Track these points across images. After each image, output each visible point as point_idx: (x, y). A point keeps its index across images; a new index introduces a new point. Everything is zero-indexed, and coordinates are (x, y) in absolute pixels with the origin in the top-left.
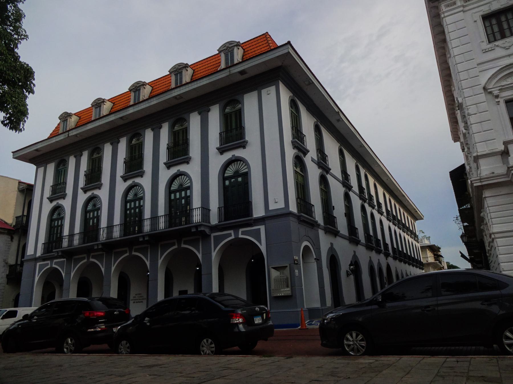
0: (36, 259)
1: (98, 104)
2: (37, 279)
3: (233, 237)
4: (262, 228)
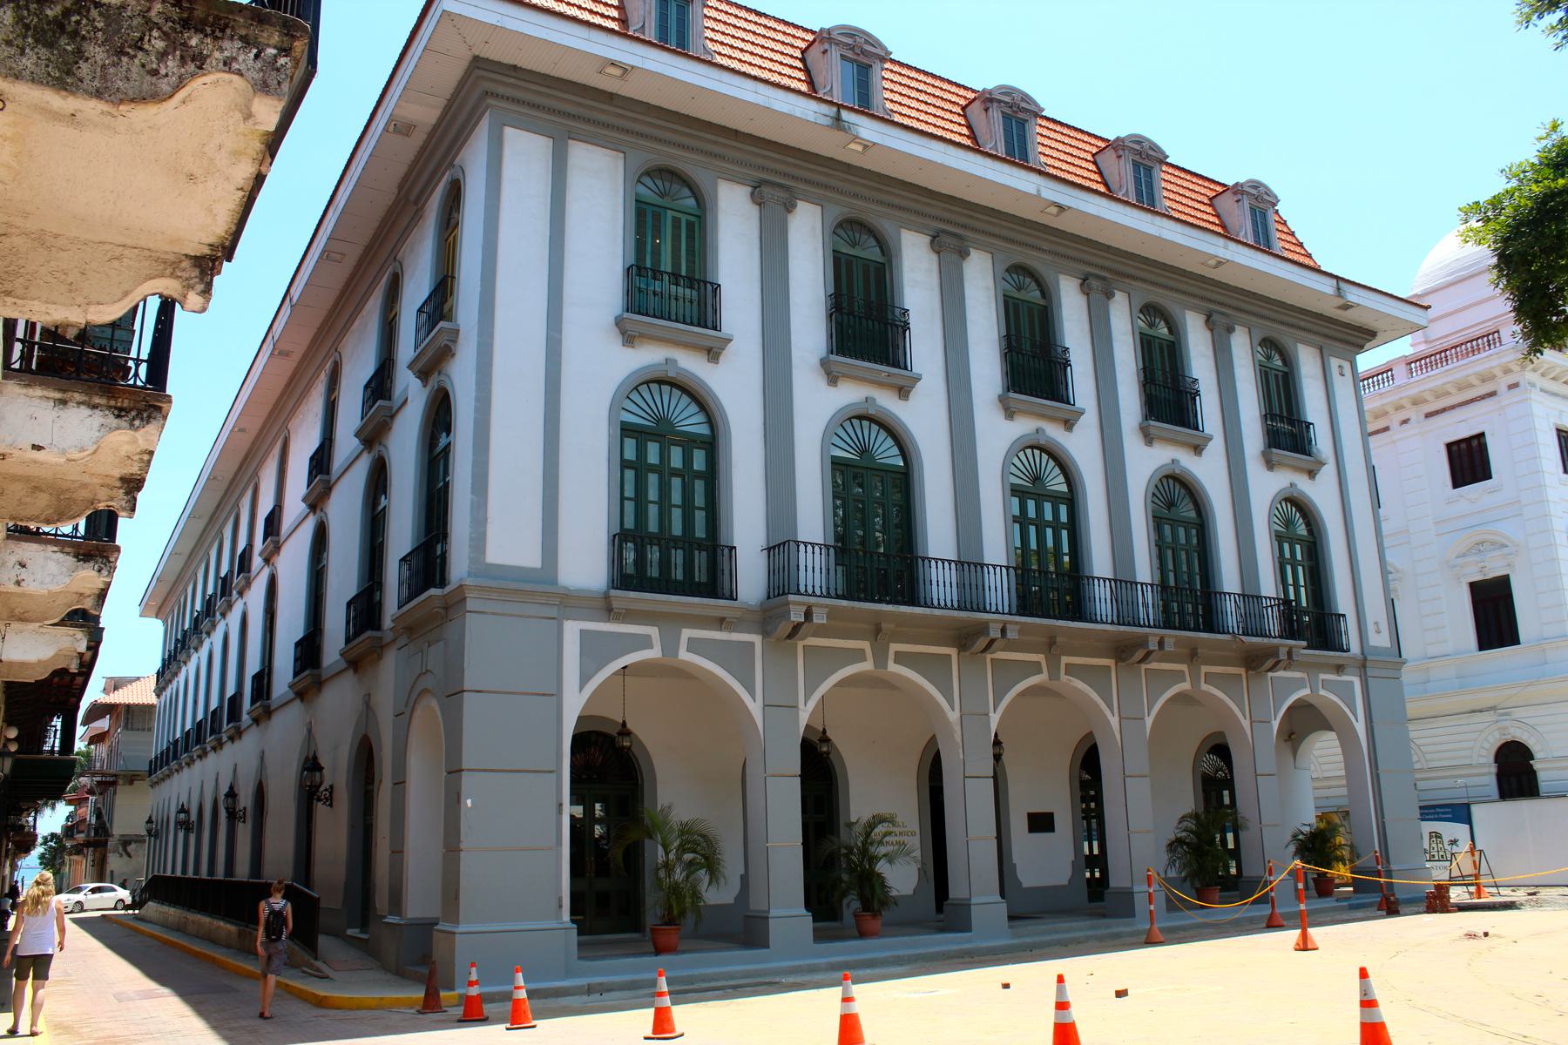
0: (571, 603)
2: (574, 704)
3: (1304, 693)
4: (1357, 682)
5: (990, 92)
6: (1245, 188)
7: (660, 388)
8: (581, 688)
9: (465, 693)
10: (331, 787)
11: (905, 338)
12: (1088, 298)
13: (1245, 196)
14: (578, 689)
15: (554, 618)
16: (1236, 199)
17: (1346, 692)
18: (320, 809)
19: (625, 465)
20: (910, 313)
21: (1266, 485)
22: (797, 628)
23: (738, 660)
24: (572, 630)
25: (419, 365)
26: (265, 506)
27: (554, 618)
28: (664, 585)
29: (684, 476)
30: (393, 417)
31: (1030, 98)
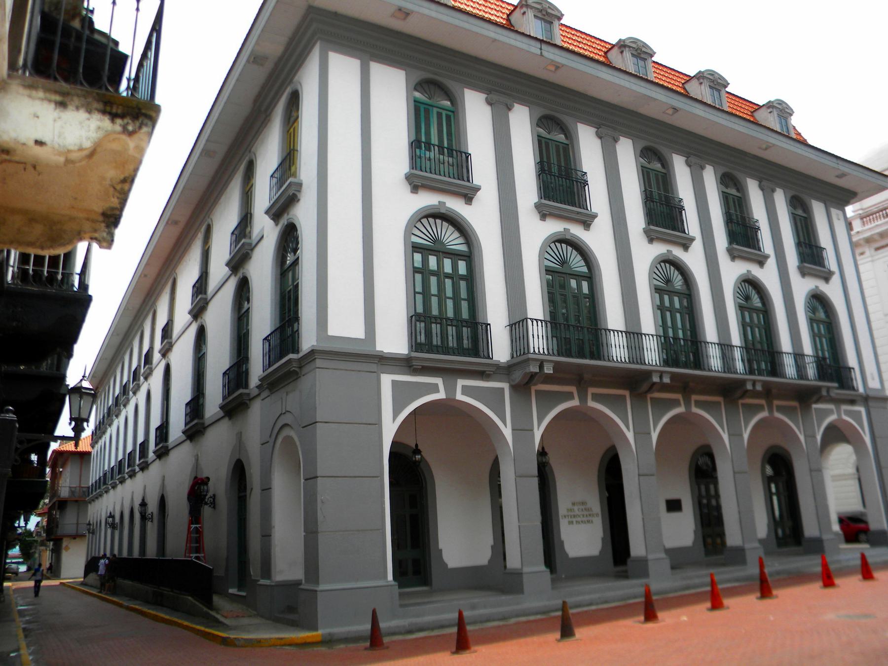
1: (544, 13)
2: (389, 430)
5: (624, 41)
6: (775, 105)
7: (435, 221)
8: (394, 420)
9: (317, 424)
10: (214, 495)
11: (585, 190)
12: (691, 169)
13: (775, 110)
14: (392, 420)
15: (375, 372)
16: (769, 111)
17: (857, 416)
18: (207, 511)
19: (416, 270)
20: (588, 174)
21: (802, 287)
22: (533, 376)
23: (494, 399)
24: (387, 380)
25: (274, 211)
26: (161, 321)
27: (375, 372)
28: (444, 349)
29: (453, 278)
30: (252, 250)
31: (647, 46)
